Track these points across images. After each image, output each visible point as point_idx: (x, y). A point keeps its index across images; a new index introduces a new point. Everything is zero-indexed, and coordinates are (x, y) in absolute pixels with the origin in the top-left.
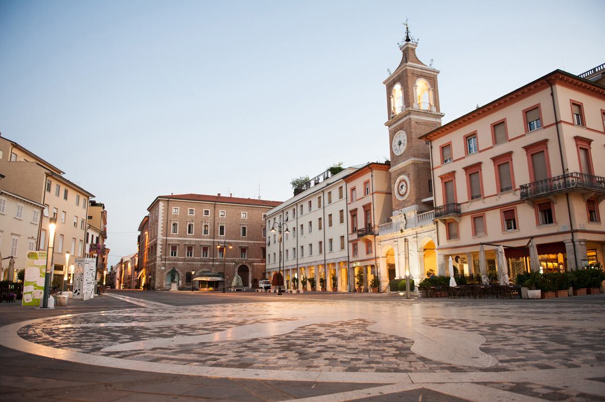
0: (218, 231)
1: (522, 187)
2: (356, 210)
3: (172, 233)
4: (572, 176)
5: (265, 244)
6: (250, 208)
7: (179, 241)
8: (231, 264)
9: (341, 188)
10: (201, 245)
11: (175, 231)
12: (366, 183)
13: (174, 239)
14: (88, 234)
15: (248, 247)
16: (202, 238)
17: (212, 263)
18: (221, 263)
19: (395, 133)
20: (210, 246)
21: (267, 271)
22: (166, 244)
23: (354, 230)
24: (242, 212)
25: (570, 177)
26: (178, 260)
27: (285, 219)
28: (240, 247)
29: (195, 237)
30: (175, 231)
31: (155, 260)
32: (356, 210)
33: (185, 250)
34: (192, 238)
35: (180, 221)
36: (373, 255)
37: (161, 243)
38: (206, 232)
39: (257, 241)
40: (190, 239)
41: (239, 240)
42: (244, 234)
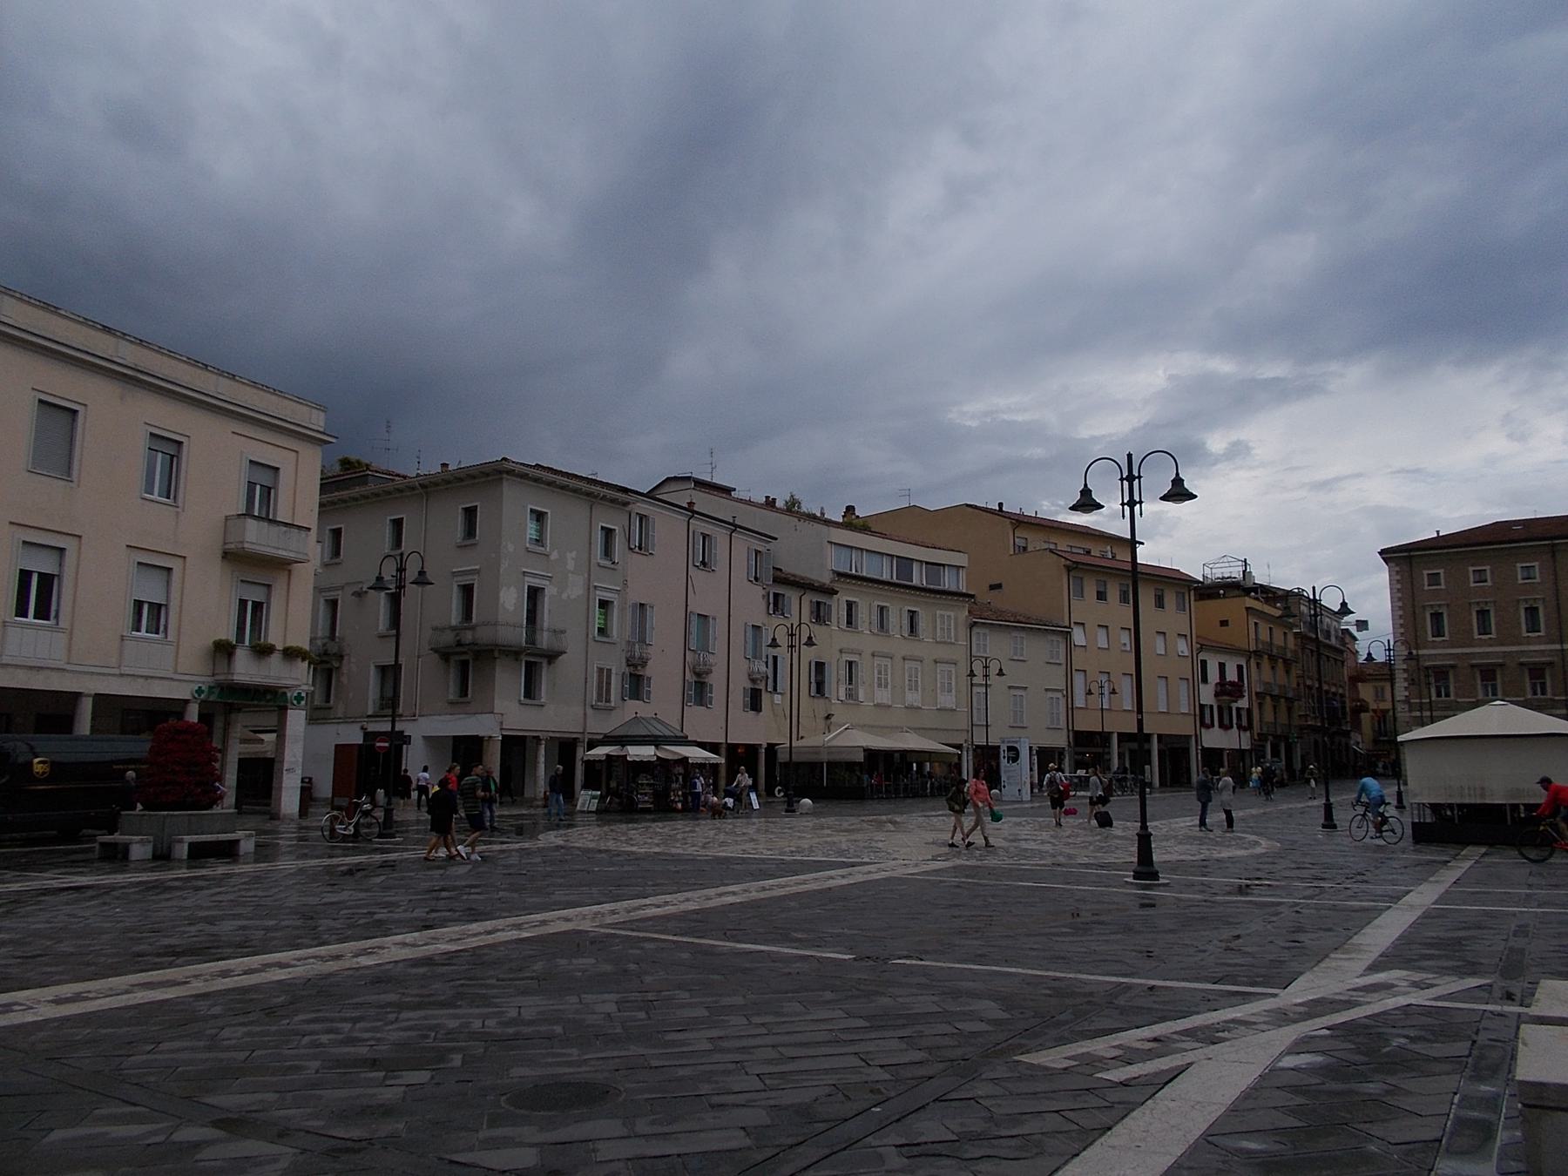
10: (1522, 664)
11: (1438, 632)
14: (1204, 663)
16: (1520, 644)
20: (1551, 664)
30: (1438, 632)
34: (1491, 646)
35: (1448, 605)
37: (1405, 667)
38: (1533, 627)
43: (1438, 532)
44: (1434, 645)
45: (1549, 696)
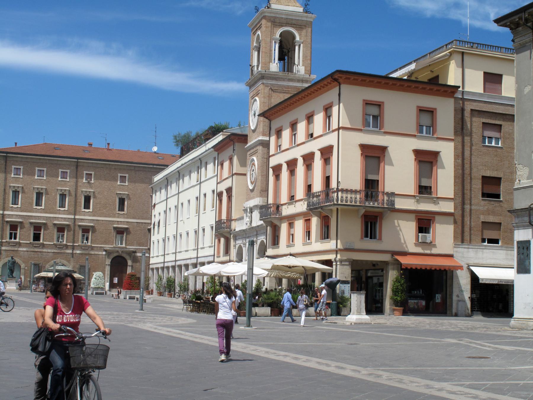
0: (81, 202)
5: (151, 223)
6: (133, 168)
8: (100, 253)
16: (56, 213)
17: (70, 251)
20: (68, 226)
21: (151, 266)
24: (119, 175)
26: (19, 244)
28: (115, 228)
29: (44, 211)
33: (30, 230)
39: (142, 219)
41: (114, 216)
42: (121, 208)
43: (16, 144)
44: (12, 209)
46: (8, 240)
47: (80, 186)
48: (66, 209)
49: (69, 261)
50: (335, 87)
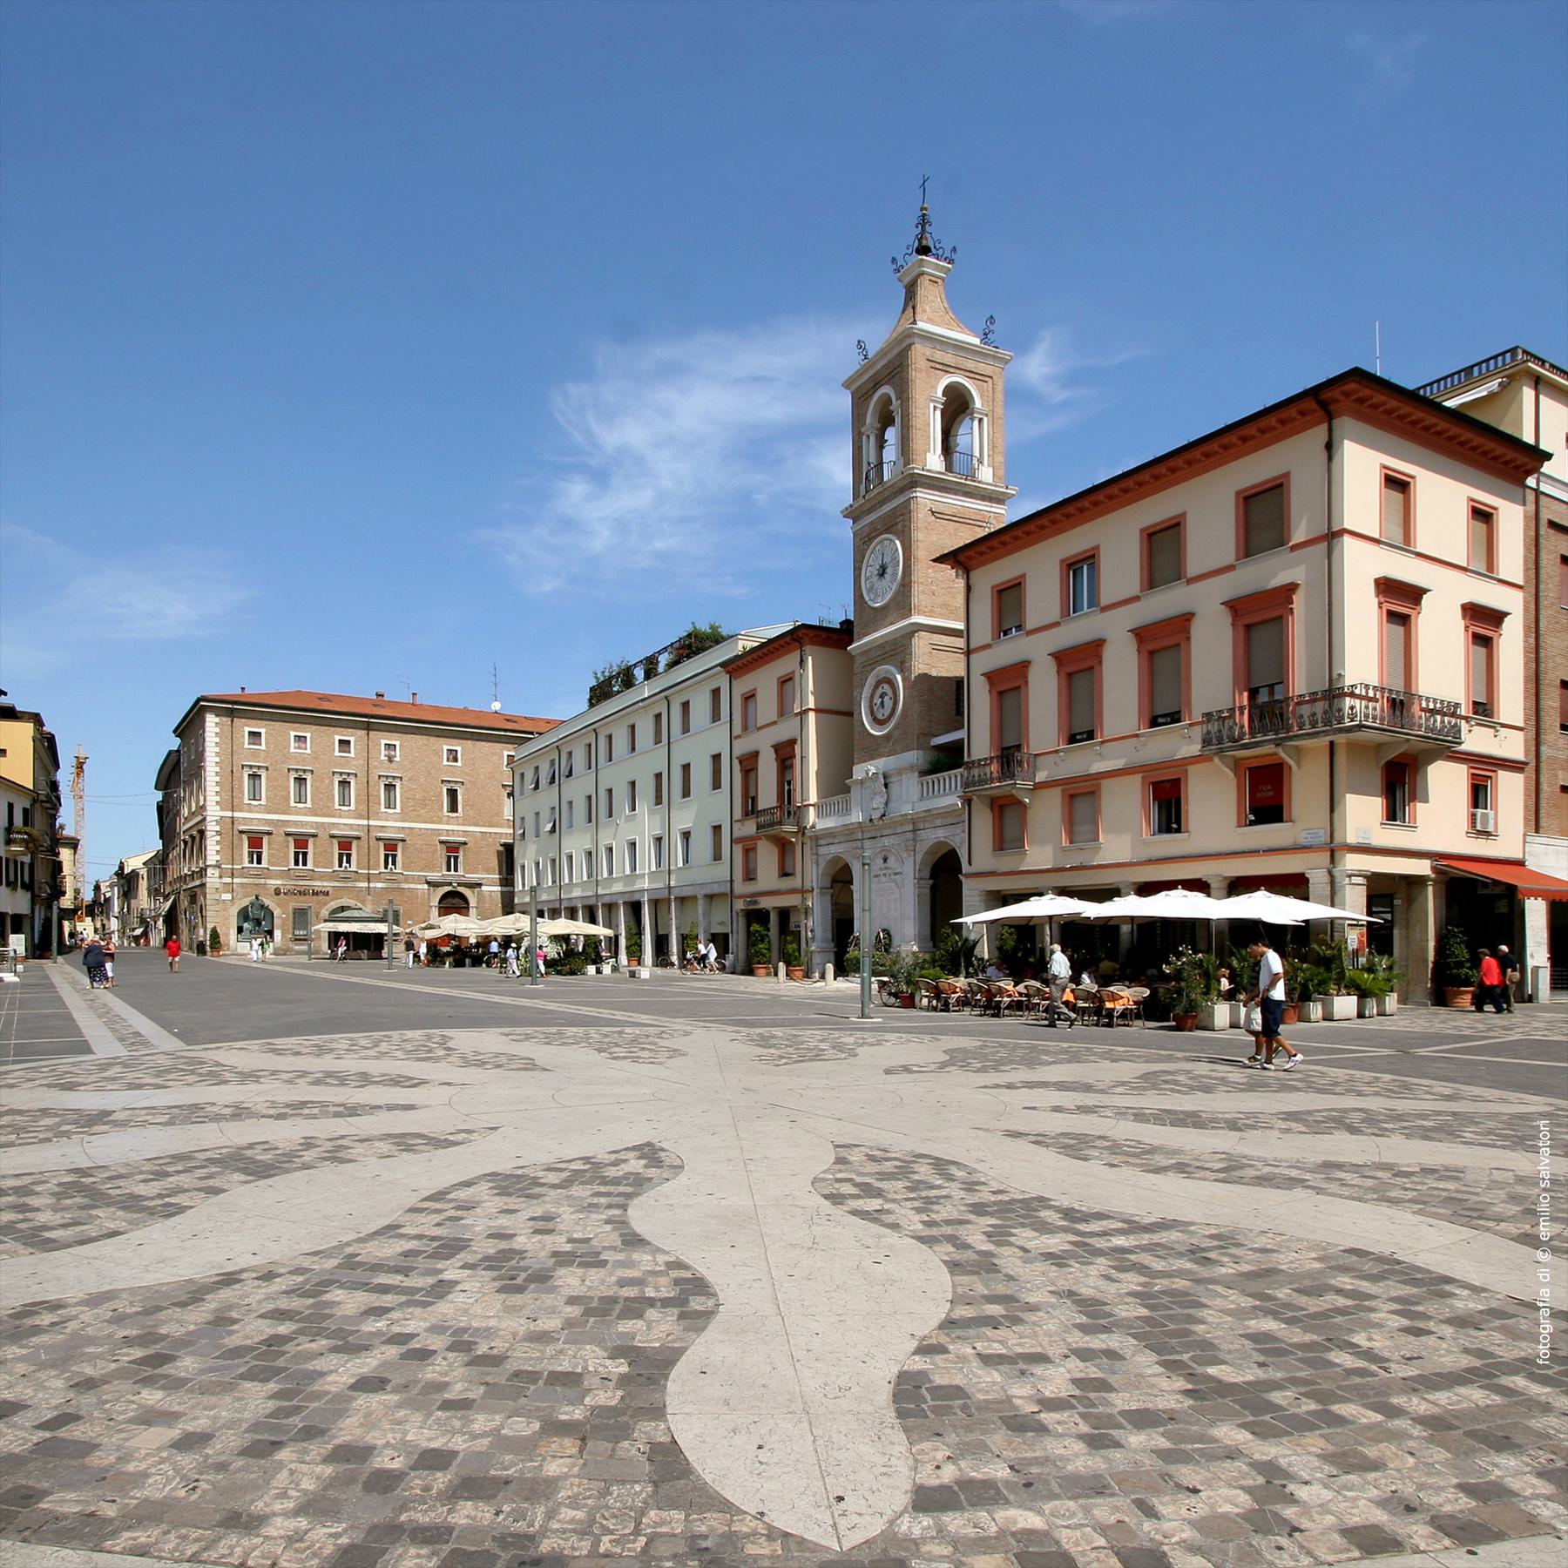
1: (1208, 716)
2: (755, 755)
3: (246, 801)
4: (1352, 695)
7: (267, 822)
8: (419, 887)
9: (716, 693)
10: (333, 837)
11: (255, 796)
12: (785, 681)
13: (254, 817)
15: (465, 843)
16: (333, 816)
17: (366, 884)
18: (390, 885)
19: (871, 540)
20: (358, 838)
22: (230, 828)
23: (750, 808)
25: (1346, 695)
27: (565, 771)
30: (255, 796)
31: (202, 872)
32: (755, 755)
36: (796, 882)
39: (490, 826)
40: (302, 819)
41: (440, 822)
42: (453, 807)
45: (354, 868)
46: (247, 864)
47: (376, 767)
48: (353, 807)
49: (363, 902)
50: (1316, 423)
